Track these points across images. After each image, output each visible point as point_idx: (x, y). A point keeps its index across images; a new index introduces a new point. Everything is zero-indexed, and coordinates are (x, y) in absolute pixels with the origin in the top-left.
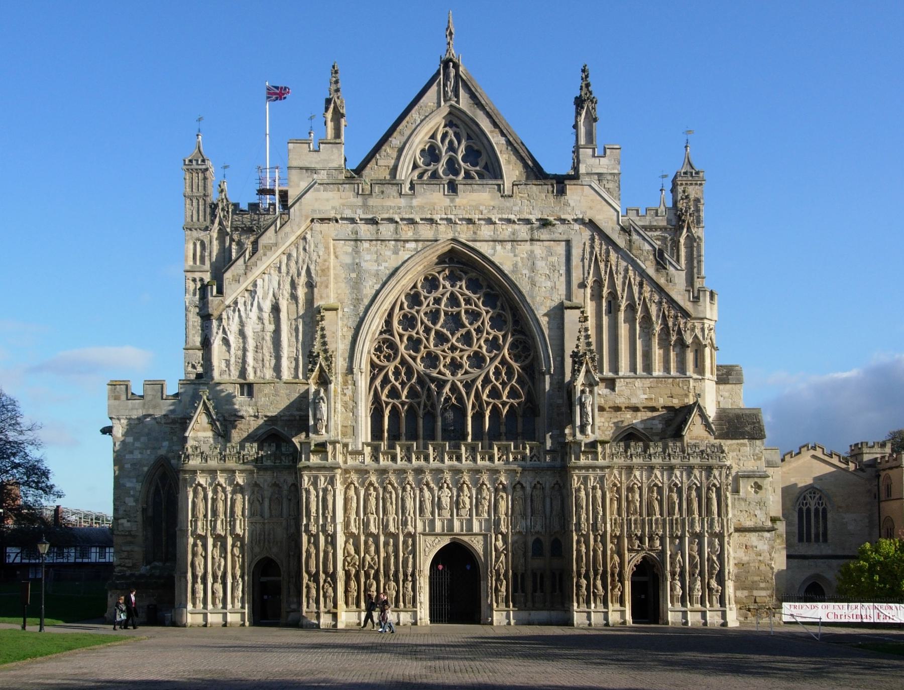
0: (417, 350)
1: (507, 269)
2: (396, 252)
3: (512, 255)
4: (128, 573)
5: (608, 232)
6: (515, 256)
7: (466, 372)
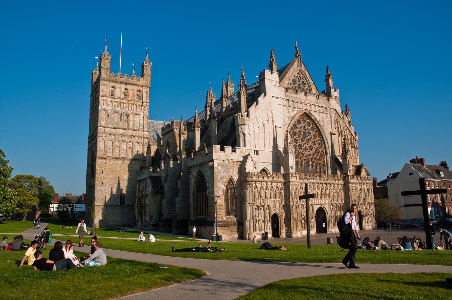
0: (297, 143)
1: (318, 120)
2: (293, 111)
3: (319, 116)
4: (220, 220)
5: (339, 113)
6: (320, 117)
7: (309, 152)
